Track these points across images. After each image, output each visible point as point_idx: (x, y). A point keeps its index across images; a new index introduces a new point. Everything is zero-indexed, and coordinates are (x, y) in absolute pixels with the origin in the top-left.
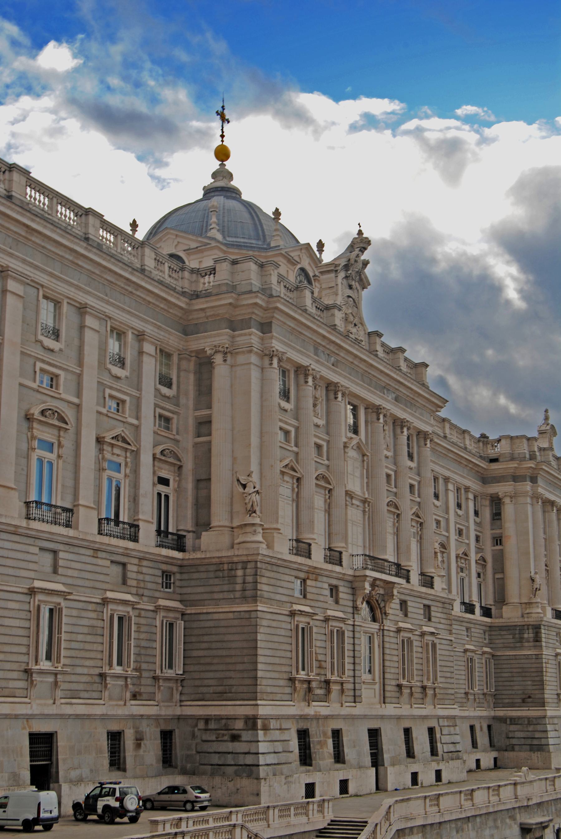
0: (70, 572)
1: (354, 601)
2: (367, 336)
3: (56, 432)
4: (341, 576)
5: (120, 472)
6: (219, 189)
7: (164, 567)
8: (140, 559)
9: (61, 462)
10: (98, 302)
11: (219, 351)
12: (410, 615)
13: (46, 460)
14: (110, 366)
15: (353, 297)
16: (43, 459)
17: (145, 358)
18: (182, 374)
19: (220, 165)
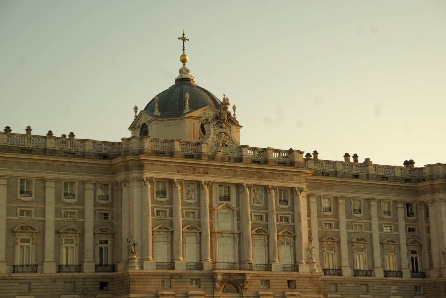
0: (38, 290)
1: (214, 285)
2: (238, 149)
3: (30, 234)
4: (200, 274)
5: (73, 243)
6: (179, 80)
7: (102, 280)
8: (84, 279)
9: (34, 246)
10: (53, 175)
11: (122, 182)
12: (271, 287)
13: (25, 246)
14: (65, 200)
15: (223, 131)
16: (24, 246)
17: (86, 192)
18: (115, 192)
19: (183, 65)
